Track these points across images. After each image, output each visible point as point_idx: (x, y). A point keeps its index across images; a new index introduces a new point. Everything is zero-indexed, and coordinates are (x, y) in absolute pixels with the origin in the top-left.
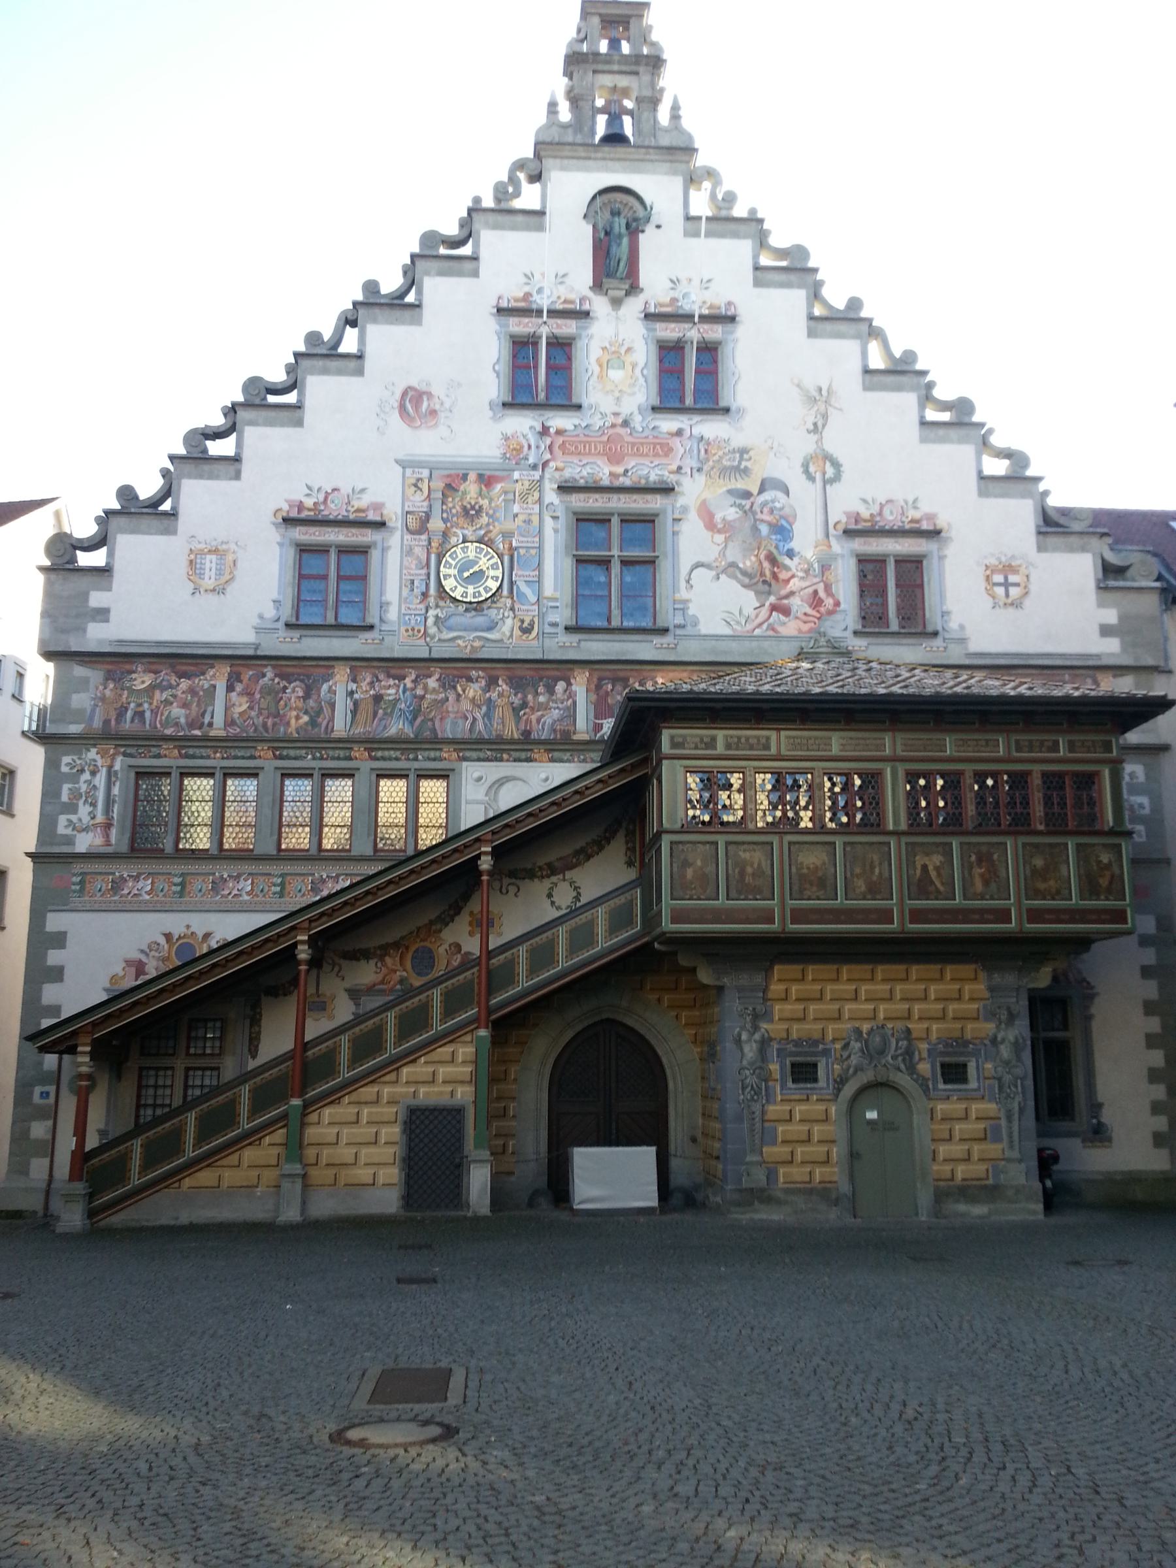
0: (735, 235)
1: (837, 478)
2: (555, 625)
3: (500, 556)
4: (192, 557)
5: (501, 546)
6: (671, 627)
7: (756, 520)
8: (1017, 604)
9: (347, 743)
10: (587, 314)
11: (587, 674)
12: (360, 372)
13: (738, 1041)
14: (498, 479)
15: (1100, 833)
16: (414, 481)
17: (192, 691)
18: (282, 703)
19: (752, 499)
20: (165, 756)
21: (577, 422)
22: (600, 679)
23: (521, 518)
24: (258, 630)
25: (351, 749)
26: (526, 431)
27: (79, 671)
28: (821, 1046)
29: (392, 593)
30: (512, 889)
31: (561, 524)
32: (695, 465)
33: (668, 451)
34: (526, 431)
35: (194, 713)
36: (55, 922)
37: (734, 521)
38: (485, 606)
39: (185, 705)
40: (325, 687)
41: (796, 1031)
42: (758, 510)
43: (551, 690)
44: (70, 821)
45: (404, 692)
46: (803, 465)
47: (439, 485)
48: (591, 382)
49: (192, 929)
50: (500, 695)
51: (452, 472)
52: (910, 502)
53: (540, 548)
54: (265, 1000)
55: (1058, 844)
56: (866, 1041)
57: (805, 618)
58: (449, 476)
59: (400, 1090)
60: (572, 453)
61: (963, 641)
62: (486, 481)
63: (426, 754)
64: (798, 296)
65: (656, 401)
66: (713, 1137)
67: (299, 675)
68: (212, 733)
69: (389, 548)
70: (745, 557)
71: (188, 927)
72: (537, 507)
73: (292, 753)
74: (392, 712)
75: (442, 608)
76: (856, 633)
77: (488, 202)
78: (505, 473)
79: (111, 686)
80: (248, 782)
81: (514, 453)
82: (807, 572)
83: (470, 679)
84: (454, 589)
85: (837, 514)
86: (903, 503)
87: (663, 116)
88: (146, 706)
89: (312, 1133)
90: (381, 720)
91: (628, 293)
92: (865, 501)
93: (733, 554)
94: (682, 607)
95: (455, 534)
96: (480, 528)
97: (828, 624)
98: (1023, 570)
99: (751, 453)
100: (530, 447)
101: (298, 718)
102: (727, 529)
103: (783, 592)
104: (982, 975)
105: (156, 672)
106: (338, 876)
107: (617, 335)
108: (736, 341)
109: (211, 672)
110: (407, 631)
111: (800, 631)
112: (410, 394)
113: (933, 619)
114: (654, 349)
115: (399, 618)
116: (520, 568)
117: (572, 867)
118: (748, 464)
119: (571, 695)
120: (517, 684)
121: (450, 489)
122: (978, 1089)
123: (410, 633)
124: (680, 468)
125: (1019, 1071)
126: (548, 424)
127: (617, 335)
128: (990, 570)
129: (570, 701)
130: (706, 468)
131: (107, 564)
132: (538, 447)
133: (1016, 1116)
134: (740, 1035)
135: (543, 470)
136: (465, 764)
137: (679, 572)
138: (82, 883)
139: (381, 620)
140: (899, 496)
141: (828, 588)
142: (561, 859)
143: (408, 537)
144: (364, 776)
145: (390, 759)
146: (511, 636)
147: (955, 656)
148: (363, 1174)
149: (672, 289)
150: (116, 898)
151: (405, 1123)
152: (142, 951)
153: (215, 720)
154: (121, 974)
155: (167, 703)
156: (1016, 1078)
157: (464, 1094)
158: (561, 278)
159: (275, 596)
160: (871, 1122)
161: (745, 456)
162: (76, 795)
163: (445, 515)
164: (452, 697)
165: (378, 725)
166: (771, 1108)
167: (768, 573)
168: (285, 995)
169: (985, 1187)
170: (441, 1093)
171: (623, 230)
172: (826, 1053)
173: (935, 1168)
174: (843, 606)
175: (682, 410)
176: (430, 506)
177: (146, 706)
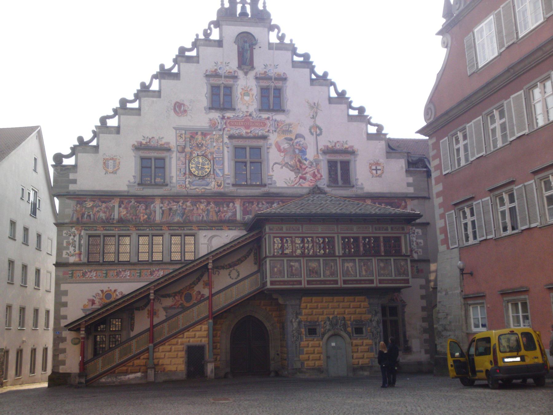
1: (321, 134)
2: (228, 184)
3: (210, 161)
4: (104, 161)
8: (380, 176)
11: (240, 200)
13: (291, 322)
14: (209, 134)
15: (402, 256)
16: (179, 135)
17: (107, 207)
18: (138, 211)
20: (99, 230)
21: (234, 114)
22: (244, 202)
23: (216, 147)
24: (128, 186)
25: (162, 226)
26: (217, 118)
27: (68, 201)
28: (317, 323)
30: (217, 273)
32: (274, 129)
33: (265, 125)
34: (217, 118)
38: (205, 177)
39: (105, 212)
40: (152, 205)
44: (67, 253)
47: (188, 136)
48: (238, 101)
49: (110, 289)
50: (211, 208)
53: (223, 158)
54: (136, 312)
55: (389, 259)
58: (191, 133)
59: (184, 340)
60: (233, 125)
61: (362, 188)
62: (204, 135)
64: (307, 71)
66: (284, 353)
69: (172, 158)
71: (109, 288)
72: (221, 144)
73: (142, 228)
74: (175, 214)
75: (191, 178)
78: (210, 132)
80: (127, 238)
81: (213, 125)
82: (311, 165)
83: (201, 202)
85: (321, 146)
88: (91, 213)
90: (172, 216)
91: (250, 70)
92: (330, 142)
93: (287, 160)
94: (271, 177)
95: (194, 153)
96: (203, 151)
99: (293, 125)
101: (143, 216)
103: (304, 172)
105: (94, 201)
107: (247, 84)
109: (113, 201)
113: (352, 179)
117: (236, 265)
118: (291, 129)
119: (235, 208)
120: (217, 204)
121: (192, 137)
124: (269, 130)
126: (225, 115)
127: (247, 84)
129: (234, 210)
130: (277, 130)
132: (221, 123)
134: (292, 320)
136: (200, 231)
141: (318, 171)
143: (178, 154)
144: (167, 236)
145: (175, 230)
146: (214, 188)
148: (173, 368)
150: (84, 278)
151: (186, 351)
152: (94, 296)
155: (98, 212)
158: (227, 64)
159: (134, 174)
161: (290, 127)
164: (195, 208)
166: (302, 343)
167: (298, 166)
168: (142, 310)
169: (368, 366)
174: (323, 177)
175: (269, 110)
177: (91, 213)
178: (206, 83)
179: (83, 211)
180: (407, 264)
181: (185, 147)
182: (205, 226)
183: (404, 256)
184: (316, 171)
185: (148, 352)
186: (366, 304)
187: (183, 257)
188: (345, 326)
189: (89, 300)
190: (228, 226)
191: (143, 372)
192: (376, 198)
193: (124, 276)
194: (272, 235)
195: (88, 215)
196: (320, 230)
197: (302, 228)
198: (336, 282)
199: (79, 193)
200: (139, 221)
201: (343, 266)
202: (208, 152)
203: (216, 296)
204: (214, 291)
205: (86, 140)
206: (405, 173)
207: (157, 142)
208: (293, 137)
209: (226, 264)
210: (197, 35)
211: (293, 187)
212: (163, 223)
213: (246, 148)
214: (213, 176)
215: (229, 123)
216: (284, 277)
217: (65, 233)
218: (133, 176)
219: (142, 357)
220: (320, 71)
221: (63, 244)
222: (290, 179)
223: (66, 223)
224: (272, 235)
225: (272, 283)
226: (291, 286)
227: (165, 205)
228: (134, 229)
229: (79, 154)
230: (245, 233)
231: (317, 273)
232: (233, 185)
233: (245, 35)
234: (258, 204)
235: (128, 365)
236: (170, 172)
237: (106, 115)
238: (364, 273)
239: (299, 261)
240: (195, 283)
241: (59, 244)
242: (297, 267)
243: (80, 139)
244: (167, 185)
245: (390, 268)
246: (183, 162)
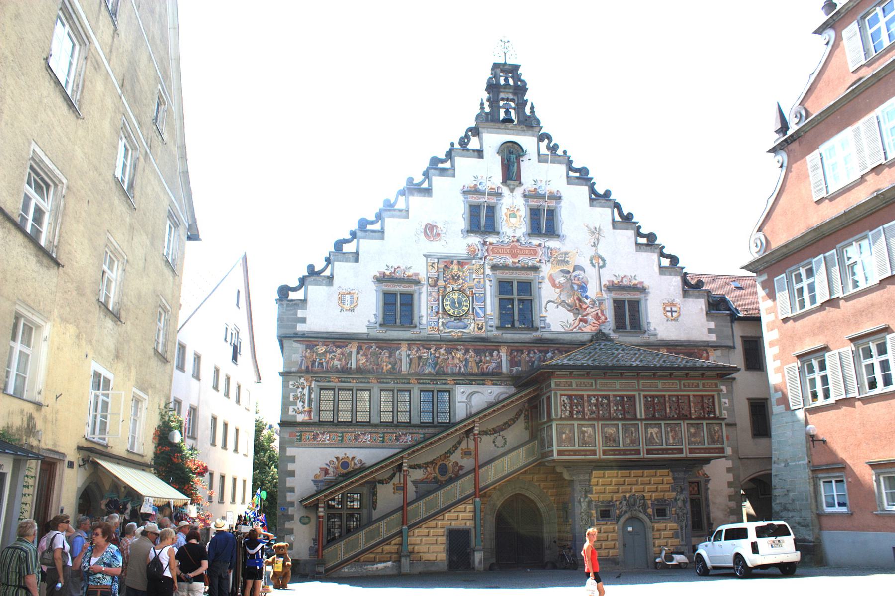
1: (604, 266)
2: (491, 326)
3: (468, 297)
4: (340, 295)
5: (468, 292)
7: (572, 283)
8: (676, 320)
10: (501, 194)
12: (407, 217)
13: (580, 502)
16: (431, 264)
17: (342, 354)
18: (380, 359)
21: (498, 239)
22: (512, 350)
24: (368, 327)
26: (477, 243)
28: (611, 503)
29: (424, 311)
33: (536, 253)
34: (477, 243)
35: (343, 363)
38: (463, 318)
39: (340, 360)
40: (397, 352)
41: (602, 497)
43: (491, 355)
44: (294, 409)
45: (431, 354)
47: (441, 265)
48: (503, 224)
52: (633, 276)
53: (484, 294)
58: (446, 262)
61: (656, 335)
62: (461, 264)
65: (529, 231)
67: (386, 347)
69: (422, 292)
70: (568, 298)
71: (345, 454)
72: (482, 275)
73: (385, 381)
75: (445, 319)
79: (309, 351)
81: (472, 253)
82: (593, 305)
83: (458, 350)
84: (450, 310)
85: (604, 281)
87: (527, 111)
88: (323, 360)
90: (422, 367)
91: (517, 186)
92: (615, 276)
93: (564, 297)
94: (544, 319)
95: (449, 287)
96: (459, 285)
97: (603, 327)
98: (677, 305)
100: (479, 250)
101: (387, 366)
103: (584, 314)
104: (671, 474)
105: (327, 346)
106: (406, 433)
107: (513, 203)
108: (561, 207)
111: (592, 330)
116: (477, 302)
117: (502, 430)
118: (568, 259)
119: (500, 357)
120: (478, 352)
121: (446, 267)
124: (541, 260)
125: (685, 511)
126: (486, 240)
127: (513, 203)
129: (499, 360)
130: (551, 260)
132: (482, 250)
133: (684, 528)
134: (580, 499)
136: (457, 386)
139: (420, 323)
140: (629, 274)
141: (602, 312)
142: (498, 426)
143: (430, 288)
145: (426, 384)
146: (474, 331)
148: (431, 557)
151: (447, 536)
152: (327, 465)
154: (319, 474)
155: (332, 359)
156: (684, 514)
159: (375, 313)
160: (630, 532)
161: (567, 256)
164: (451, 357)
167: (578, 305)
170: (461, 524)
171: (515, 160)
173: (655, 549)
174: (608, 320)
177: (323, 360)
178: (464, 201)
180: (722, 429)
181: (437, 279)
182: (463, 380)
183: (718, 418)
185: (402, 537)
186: (670, 479)
187: (395, 418)
188: (645, 506)
189: (321, 469)
190: (492, 381)
191: (394, 562)
192: (673, 346)
193: (364, 440)
194: (559, 393)
195: (319, 363)
196: (618, 387)
197: (638, 384)
198: (638, 452)
199: (310, 335)
200: (382, 371)
201: (646, 432)
202: (466, 286)
203: (483, 469)
204: (481, 462)
205: (316, 269)
206: (705, 316)
207: (404, 273)
208: (571, 270)
209: (490, 427)
210: (452, 144)
211: (571, 332)
212: (412, 375)
213: (512, 282)
214: (472, 316)
216: (574, 446)
217: (292, 385)
219: (393, 542)
220: (600, 190)
221: (289, 398)
223: (294, 372)
224: (559, 393)
225: (560, 453)
226: (583, 457)
227: (414, 352)
228: (376, 381)
229: (309, 286)
230: (512, 390)
231: (615, 441)
232: (497, 328)
233: (510, 144)
234: (529, 353)
235: (375, 551)
236: (419, 312)
237: (342, 239)
238: (671, 441)
239: (593, 426)
240: (450, 452)
241: (285, 398)
242: (590, 434)
243: (311, 268)
244: (415, 327)
245: (702, 434)
246: (435, 298)
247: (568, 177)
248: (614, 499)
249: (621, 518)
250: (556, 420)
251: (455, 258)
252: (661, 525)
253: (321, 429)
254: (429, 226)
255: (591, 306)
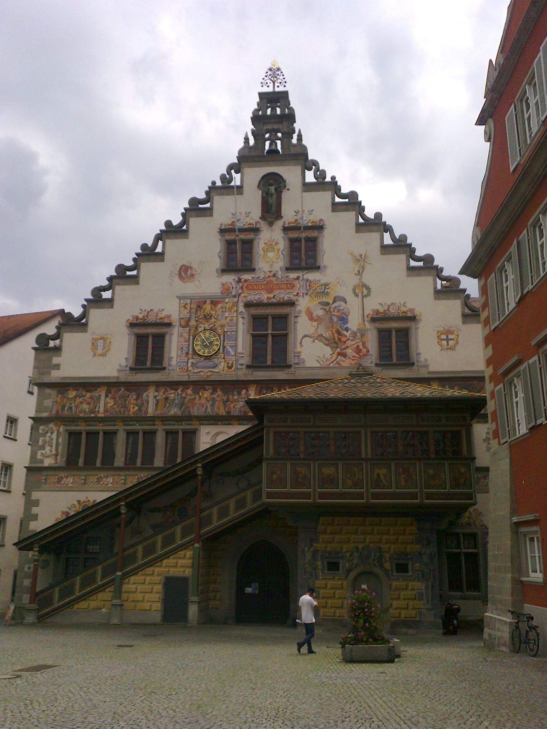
0: (324, 190)
1: (368, 295)
2: (242, 365)
6: (293, 365)
7: (331, 315)
8: (452, 349)
9: (153, 419)
12: (163, 260)
13: (303, 551)
16: (184, 305)
17: (91, 398)
18: (127, 402)
19: (330, 306)
21: (253, 276)
22: (261, 388)
23: (229, 318)
24: (119, 371)
26: (231, 281)
27: (48, 391)
31: (246, 321)
32: (305, 292)
33: (293, 286)
34: (231, 281)
35: (92, 407)
36: (35, 495)
37: (322, 316)
38: (213, 357)
39: (89, 404)
40: (145, 394)
42: (332, 311)
43: (239, 394)
44: (42, 453)
45: (178, 395)
46: (353, 290)
47: (194, 306)
48: (260, 258)
49: (89, 499)
50: (218, 396)
51: (200, 300)
52: (402, 303)
53: (236, 332)
56: (361, 553)
57: (353, 358)
58: (199, 302)
60: (251, 290)
61: (427, 366)
62: (214, 303)
63: (186, 422)
68: (99, 415)
69: (173, 334)
71: (87, 498)
72: (235, 314)
73: (131, 423)
74: (172, 404)
76: (377, 365)
77: (219, 183)
81: (226, 290)
82: (354, 337)
83: (205, 390)
84: (199, 350)
85: (368, 311)
86: (399, 305)
87: (294, 141)
88: (73, 404)
89: (125, 587)
92: (381, 304)
93: (321, 331)
94: (298, 355)
95: (201, 327)
96: (211, 324)
98: (455, 332)
99: (330, 285)
100: (233, 287)
101: (133, 408)
102: (318, 319)
103: (343, 347)
107: (271, 238)
108: (323, 236)
109: (99, 389)
110: (180, 369)
111: (351, 364)
112: (184, 268)
114: (287, 242)
115: (177, 364)
118: (328, 290)
120: (225, 392)
121: (199, 307)
122: (412, 576)
123: (181, 370)
124: (298, 293)
126: (240, 277)
127: (271, 238)
128: (440, 333)
130: (309, 293)
131: (60, 345)
132: (236, 288)
134: (304, 548)
135: (238, 298)
136: (202, 426)
137: (297, 340)
138: (46, 479)
140: (397, 301)
141: (364, 344)
143: (182, 329)
146: (223, 370)
147: (423, 373)
149: (296, 215)
152: (69, 508)
153: (100, 410)
157: (188, 572)
158: (248, 214)
159: (126, 356)
161: (327, 287)
162: (45, 442)
163: (196, 319)
164: (197, 397)
165: (166, 411)
167: (336, 338)
172: (342, 558)
174: (370, 352)
176: (190, 316)
178: (220, 240)
179: (65, 402)
181: (189, 320)
184: (361, 343)
193: (106, 483)
194: (272, 430)
202: (217, 325)
207: (156, 316)
210: (214, 183)
211: (328, 367)
214: (223, 355)
215: (247, 287)
218: (126, 358)
220: (370, 213)
221: (38, 443)
222: (324, 355)
227: (161, 393)
236: (170, 353)
238: (403, 483)
244: (164, 368)
246: (186, 339)
247: (334, 204)
248: (344, 550)
249: (351, 573)
250: (266, 459)
251: (209, 297)
252: (401, 583)
253: (66, 473)
254: (184, 268)
255: (351, 338)
